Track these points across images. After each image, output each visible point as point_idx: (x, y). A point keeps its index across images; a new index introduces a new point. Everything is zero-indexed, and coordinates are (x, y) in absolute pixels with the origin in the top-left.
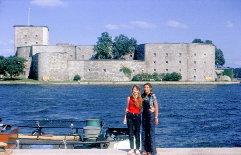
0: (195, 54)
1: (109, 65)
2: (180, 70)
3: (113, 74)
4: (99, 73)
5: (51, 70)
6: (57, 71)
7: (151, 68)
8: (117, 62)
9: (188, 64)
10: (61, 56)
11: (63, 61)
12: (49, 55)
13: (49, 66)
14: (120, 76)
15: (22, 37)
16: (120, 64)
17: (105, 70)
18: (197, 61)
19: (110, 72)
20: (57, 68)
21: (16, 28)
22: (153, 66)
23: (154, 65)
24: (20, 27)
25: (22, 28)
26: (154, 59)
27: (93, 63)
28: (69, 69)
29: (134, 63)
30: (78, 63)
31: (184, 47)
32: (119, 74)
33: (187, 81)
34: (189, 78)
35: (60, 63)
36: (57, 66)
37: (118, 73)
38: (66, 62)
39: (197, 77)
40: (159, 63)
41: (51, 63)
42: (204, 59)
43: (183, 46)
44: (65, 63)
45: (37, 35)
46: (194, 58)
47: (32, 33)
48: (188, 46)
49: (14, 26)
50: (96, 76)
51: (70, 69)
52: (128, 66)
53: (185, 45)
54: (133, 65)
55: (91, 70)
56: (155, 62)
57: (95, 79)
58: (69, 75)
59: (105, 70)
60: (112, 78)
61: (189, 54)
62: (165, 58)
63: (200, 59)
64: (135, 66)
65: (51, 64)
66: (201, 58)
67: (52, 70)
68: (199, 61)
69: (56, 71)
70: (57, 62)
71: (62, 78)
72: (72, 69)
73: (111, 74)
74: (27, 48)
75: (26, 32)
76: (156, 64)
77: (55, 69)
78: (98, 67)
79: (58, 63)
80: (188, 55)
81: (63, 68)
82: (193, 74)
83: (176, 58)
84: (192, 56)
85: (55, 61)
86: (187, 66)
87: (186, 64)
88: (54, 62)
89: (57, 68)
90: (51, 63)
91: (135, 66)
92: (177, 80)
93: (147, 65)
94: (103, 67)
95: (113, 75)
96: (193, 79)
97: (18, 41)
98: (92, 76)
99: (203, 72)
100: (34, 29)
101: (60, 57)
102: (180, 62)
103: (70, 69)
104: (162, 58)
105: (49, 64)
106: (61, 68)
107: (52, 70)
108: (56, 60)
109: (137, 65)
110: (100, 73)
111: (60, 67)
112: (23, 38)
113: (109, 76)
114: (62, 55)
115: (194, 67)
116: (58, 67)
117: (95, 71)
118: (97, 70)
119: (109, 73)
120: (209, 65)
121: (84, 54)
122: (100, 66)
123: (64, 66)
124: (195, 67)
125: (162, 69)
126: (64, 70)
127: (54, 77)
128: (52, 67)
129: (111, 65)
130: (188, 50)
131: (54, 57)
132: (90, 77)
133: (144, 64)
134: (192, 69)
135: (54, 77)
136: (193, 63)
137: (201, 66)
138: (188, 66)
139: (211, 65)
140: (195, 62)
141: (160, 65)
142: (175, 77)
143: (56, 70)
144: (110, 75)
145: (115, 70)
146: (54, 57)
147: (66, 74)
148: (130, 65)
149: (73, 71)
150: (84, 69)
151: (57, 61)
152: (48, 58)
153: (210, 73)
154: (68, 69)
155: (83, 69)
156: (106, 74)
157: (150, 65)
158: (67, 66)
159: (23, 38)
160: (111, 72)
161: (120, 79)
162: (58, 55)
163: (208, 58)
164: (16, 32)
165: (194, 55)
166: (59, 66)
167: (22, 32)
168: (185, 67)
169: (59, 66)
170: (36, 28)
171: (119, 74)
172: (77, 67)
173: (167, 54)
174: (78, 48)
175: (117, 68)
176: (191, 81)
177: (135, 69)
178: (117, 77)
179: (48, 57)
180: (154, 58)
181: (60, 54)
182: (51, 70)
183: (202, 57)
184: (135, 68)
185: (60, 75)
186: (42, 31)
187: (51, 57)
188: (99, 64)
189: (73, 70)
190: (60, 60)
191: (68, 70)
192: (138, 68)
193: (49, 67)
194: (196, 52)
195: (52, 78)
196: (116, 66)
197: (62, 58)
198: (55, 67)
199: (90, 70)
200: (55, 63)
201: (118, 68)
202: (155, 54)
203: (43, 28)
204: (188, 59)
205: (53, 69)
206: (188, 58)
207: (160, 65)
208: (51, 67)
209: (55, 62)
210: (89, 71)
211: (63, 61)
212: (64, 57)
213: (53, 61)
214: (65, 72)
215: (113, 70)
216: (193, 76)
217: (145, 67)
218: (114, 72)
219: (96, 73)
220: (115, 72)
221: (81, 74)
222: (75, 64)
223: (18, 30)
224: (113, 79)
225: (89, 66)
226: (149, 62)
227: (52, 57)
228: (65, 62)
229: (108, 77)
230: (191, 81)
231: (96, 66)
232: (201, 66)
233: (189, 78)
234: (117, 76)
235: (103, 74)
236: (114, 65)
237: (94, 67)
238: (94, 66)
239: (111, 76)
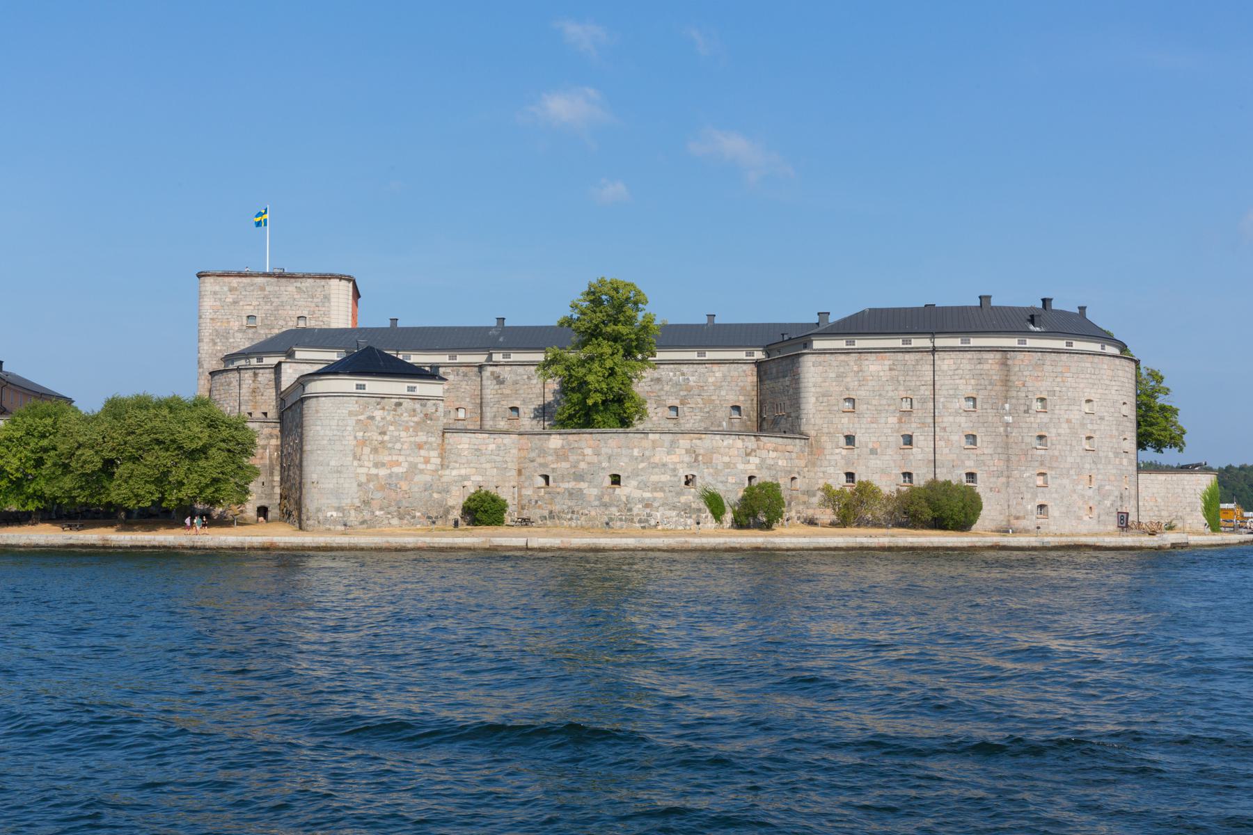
1: (636, 452)
2: (971, 476)
3: (655, 499)
4: (591, 492)
5: (363, 479)
6: (394, 481)
7: (831, 470)
8: (672, 442)
9: (1006, 447)
10: (414, 410)
11: (422, 437)
12: (355, 408)
13: (355, 457)
15: (235, 325)
16: (687, 451)
17: (616, 480)
18: (1051, 434)
19: (638, 488)
20: (396, 470)
21: (209, 284)
22: (843, 457)
23: (844, 452)
24: (226, 279)
25: (235, 281)
26: (846, 424)
27: (563, 447)
28: (452, 474)
29: (755, 446)
30: (490, 444)
31: (986, 367)
32: (683, 499)
33: (1004, 531)
34: (1017, 518)
35: (405, 447)
36: (395, 458)
37: (679, 494)
38: (435, 440)
39: (1053, 511)
40: (870, 446)
41: (363, 443)
42: (1083, 425)
43: (980, 362)
44: (431, 444)
45: (305, 313)
46: (1037, 421)
47: (282, 304)
48: (1004, 364)
49: (200, 276)
50: (576, 509)
51: (454, 473)
52: (726, 459)
53: (991, 355)
54: (748, 455)
55: (551, 479)
56: (850, 439)
57: (571, 519)
58: (451, 503)
59: (616, 480)
60: (649, 515)
61: (1014, 401)
62: (900, 421)
63: (1065, 426)
64: (757, 461)
65: (367, 450)
66: (1069, 421)
67: (370, 478)
68: (1059, 435)
69: (389, 485)
70: (398, 439)
71: (418, 514)
72: (463, 472)
73: (647, 495)
74: (255, 375)
75: (255, 303)
76: (856, 451)
77: (383, 472)
78: (583, 465)
79: (398, 446)
80: (1007, 406)
81: (421, 466)
82: (1035, 496)
83: (951, 419)
84: (1026, 412)
85: (384, 433)
86: (1003, 457)
87: (999, 450)
88: (380, 438)
89: (396, 470)
90: (363, 443)
91: (754, 460)
92: (963, 526)
93: (811, 453)
94: (605, 464)
95: (656, 504)
96: (1029, 523)
97: (215, 344)
98: (556, 508)
99: (1080, 487)
100: (290, 287)
101: (405, 417)
102: (972, 438)
103: (454, 473)
104: (883, 420)
105: (358, 451)
106: (413, 468)
107: (369, 481)
108: (391, 428)
109: (764, 453)
110: (595, 491)
111: (405, 465)
112: (239, 330)
113: (637, 509)
114: (417, 406)
115: (1037, 464)
116: (398, 464)
117: (571, 485)
118: (579, 477)
119: (637, 494)
120: (1111, 455)
121: (517, 404)
122: (595, 459)
123: (427, 461)
124: (1042, 464)
125: (883, 472)
126: (428, 478)
127: (377, 513)
128: (371, 464)
129: (647, 453)
130: (1006, 382)
131: (378, 414)
132: (546, 513)
133: (797, 449)
135: (381, 509)
136: (1036, 443)
137: (1070, 459)
138: (1008, 460)
139: (1116, 454)
141: (873, 452)
142: (945, 507)
143: (390, 476)
144: (641, 500)
145: (665, 478)
146: (378, 418)
147: (435, 495)
148: (734, 452)
149: (466, 483)
150: (520, 472)
151: (396, 433)
152: (352, 421)
153: (1117, 493)
154: (447, 472)
155: (514, 473)
156: (624, 499)
157: (826, 452)
158: (438, 461)
159: (239, 330)
160: (642, 486)
161: (689, 521)
162: (399, 404)
163: (1102, 418)
164: (208, 304)
165: (1037, 406)
166: (401, 459)
167: (235, 303)
168: (998, 464)
169: (401, 459)
170: (298, 285)
171: (683, 499)
172: (488, 465)
174: (492, 373)
175: (674, 470)
176: (1026, 531)
177: (755, 473)
178: (674, 513)
179: (351, 414)
180: (845, 420)
181: (407, 404)
182: (363, 479)
183: (1075, 416)
184: (760, 467)
185: (405, 503)
186: (327, 298)
187: (368, 414)
188: (588, 451)
189: (467, 478)
190: (407, 429)
191: (444, 479)
192: (769, 468)
193: (356, 463)
194: (1043, 388)
195: (367, 515)
196: (670, 459)
197: (416, 419)
198: (383, 465)
199: (546, 478)
200: (382, 442)
201: (678, 466)
203: (335, 282)
204: (1007, 424)
205: (374, 471)
206: (1009, 419)
207: (873, 452)
208: (366, 464)
209: (386, 438)
210: (542, 482)
211: (422, 437)
212: (426, 415)
214: (428, 488)
215: (654, 478)
216: (1031, 506)
217: (803, 463)
218: (657, 487)
219: (571, 494)
220: (662, 490)
221: (506, 494)
222: (478, 451)
223: (215, 293)
224: (653, 522)
226: (824, 438)
227: (372, 418)
228: (433, 439)
229: (630, 510)
230: (1026, 531)
231: (573, 458)
232: (1070, 459)
233: (1017, 518)
234: (674, 508)
235: (606, 499)
236: (660, 456)
237: (565, 465)
238: (566, 459)
239: (647, 506)
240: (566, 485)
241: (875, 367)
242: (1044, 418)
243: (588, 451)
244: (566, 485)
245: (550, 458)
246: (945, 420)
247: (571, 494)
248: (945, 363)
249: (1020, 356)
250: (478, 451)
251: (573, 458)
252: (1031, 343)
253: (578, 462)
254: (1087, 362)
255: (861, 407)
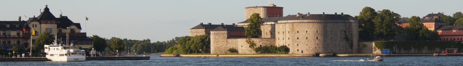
0: (298, 32)
14: (250, 51)
18: (299, 37)
25: (249, 9)
38: (225, 40)
48: (293, 25)
53: (291, 24)
96: (296, 52)
106: (222, 45)
134: (296, 44)
139: (314, 40)
140: (298, 38)
168: (292, 42)
181: (221, 35)
213: (216, 40)
216: (296, 50)
218: (246, 47)
241: (281, 26)
242: (298, 34)
246: (287, 35)
248: (287, 25)
249: (295, 24)
250: (232, 42)
252: (299, 21)
254: (306, 25)
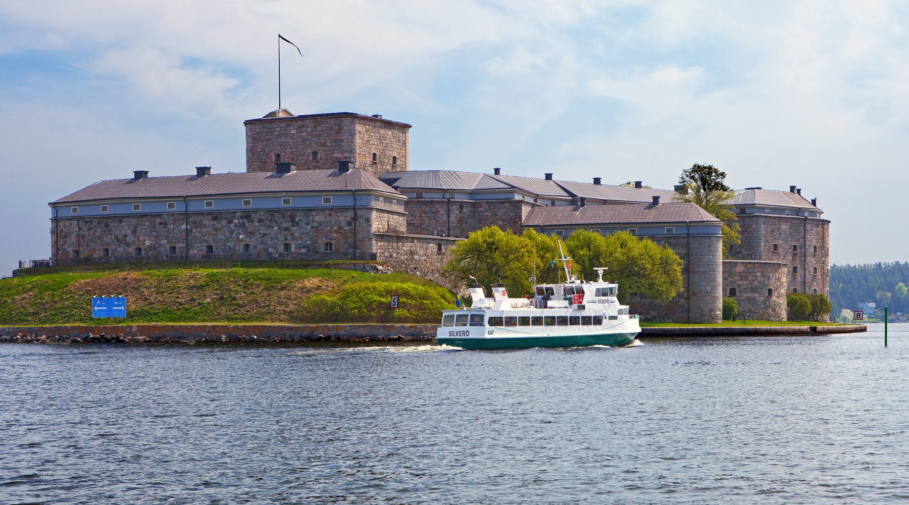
78: (756, 283)
110: (762, 299)
117: (749, 295)
118: (754, 290)
173: (795, 247)
188: (759, 274)
202: (776, 246)
219: (749, 300)
223: (360, 132)
225: (730, 279)
237: (745, 282)
240: (747, 295)
243: (759, 274)
244: (747, 295)
245: (736, 278)
247: (749, 300)
251: (750, 278)
253: (753, 281)
255: (780, 250)
